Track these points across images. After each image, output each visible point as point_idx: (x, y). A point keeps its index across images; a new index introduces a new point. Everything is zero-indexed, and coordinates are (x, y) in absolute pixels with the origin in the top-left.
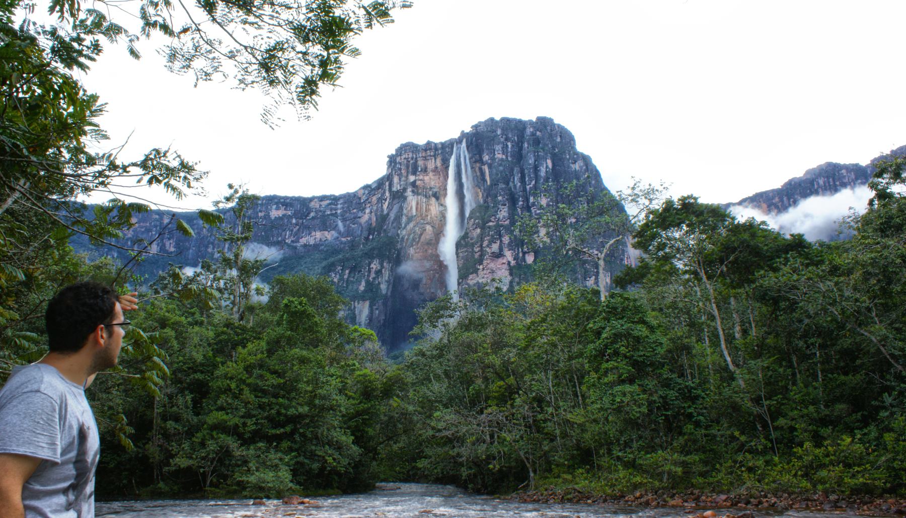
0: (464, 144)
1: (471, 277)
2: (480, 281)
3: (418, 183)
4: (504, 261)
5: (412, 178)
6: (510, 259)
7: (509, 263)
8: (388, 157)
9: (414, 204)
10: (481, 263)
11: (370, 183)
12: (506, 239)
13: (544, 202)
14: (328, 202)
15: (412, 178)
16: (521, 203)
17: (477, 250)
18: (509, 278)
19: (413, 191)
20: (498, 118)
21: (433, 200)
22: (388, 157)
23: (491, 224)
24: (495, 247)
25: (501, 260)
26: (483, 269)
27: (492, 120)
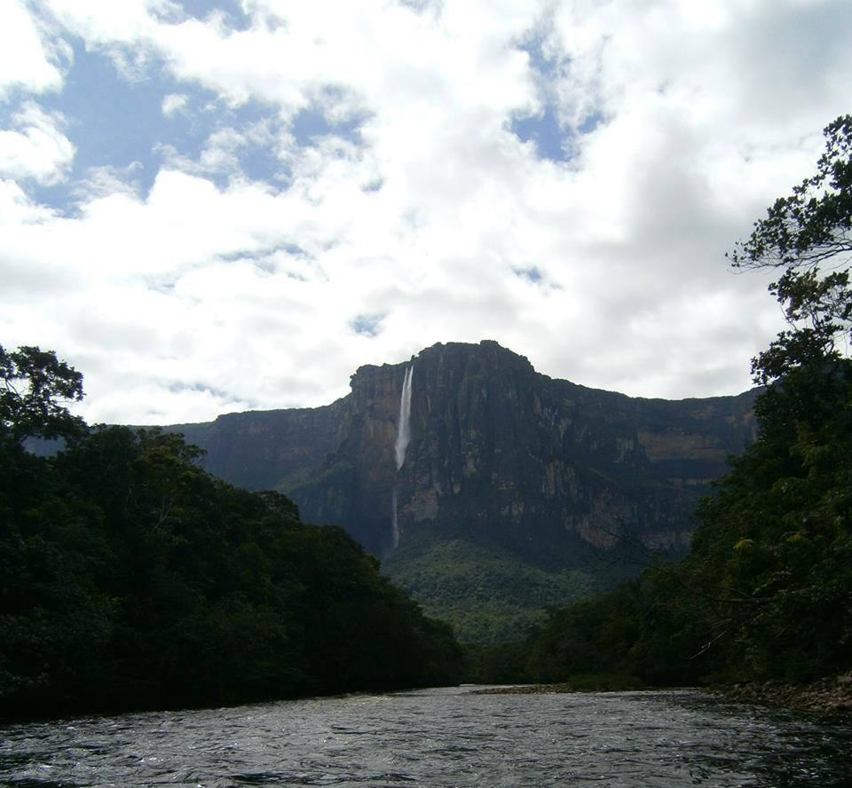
0: (412, 372)
1: (406, 506)
2: (413, 510)
3: (376, 406)
4: (434, 492)
5: (370, 402)
6: (439, 490)
7: (437, 493)
8: (351, 377)
9: (372, 428)
10: (413, 495)
11: (343, 397)
12: (435, 472)
13: (473, 434)
14: (304, 416)
15: (370, 402)
16: (451, 437)
17: (411, 481)
18: (437, 507)
19: (371, 416)
20: (444, 343)
21: (390, 423)
22: (351, 377)
23: (423, 457)
24: (425, 479)
25: (432, 491)
26: (415, 499)
27: (439, 344)
